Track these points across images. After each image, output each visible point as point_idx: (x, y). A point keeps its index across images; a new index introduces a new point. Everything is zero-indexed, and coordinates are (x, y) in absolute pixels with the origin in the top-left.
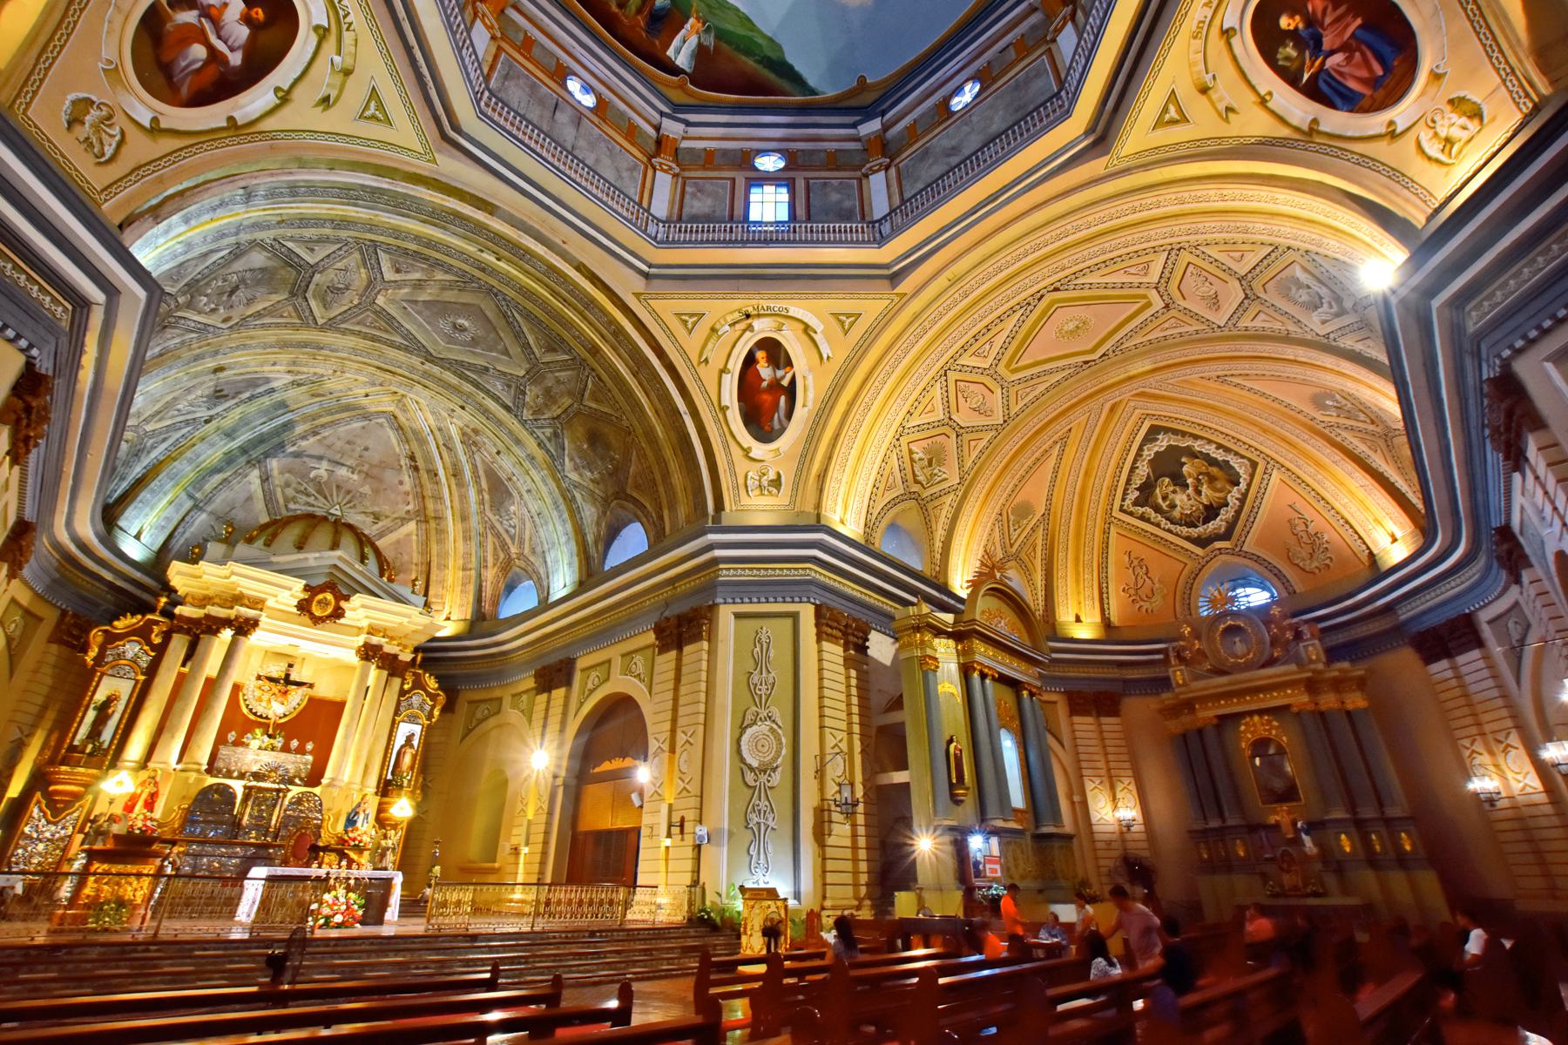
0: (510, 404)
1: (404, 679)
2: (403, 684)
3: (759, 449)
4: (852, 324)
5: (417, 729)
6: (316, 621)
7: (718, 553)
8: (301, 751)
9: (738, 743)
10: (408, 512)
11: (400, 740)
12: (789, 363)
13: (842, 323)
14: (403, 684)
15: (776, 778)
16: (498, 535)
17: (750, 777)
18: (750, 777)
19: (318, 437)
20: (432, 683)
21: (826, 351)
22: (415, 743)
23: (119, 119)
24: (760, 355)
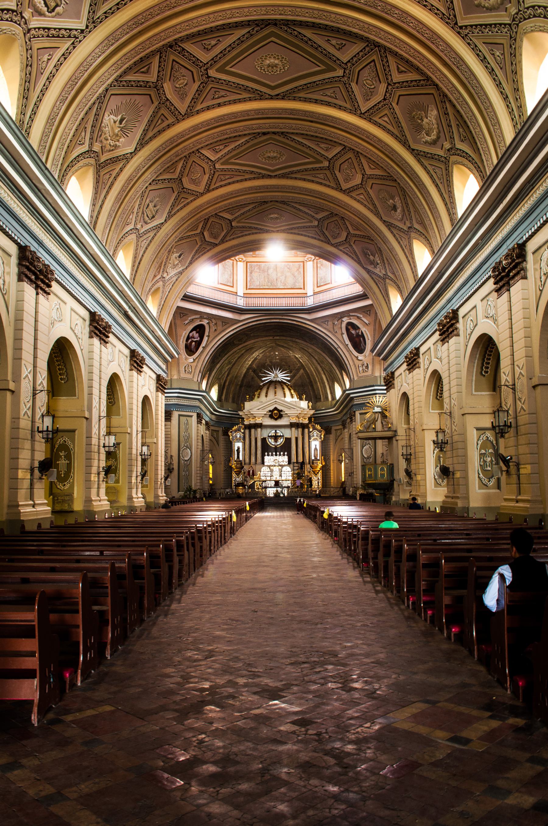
1: (309, 428)
3: (361, 357)
4: (370, 313)
6: (276, 419)
7: (352, 396)
8: (284, 455)
9: (362, 451)
11: (313, 448)
12: (359, 328)
13: (367, 313)
15: (371, 460)
16: (327, 371)
17: (365, 460)
18: (365, 460)
20: (318, 427)
21: (367, 322)
23: (190, 364)
24: (349, 327)
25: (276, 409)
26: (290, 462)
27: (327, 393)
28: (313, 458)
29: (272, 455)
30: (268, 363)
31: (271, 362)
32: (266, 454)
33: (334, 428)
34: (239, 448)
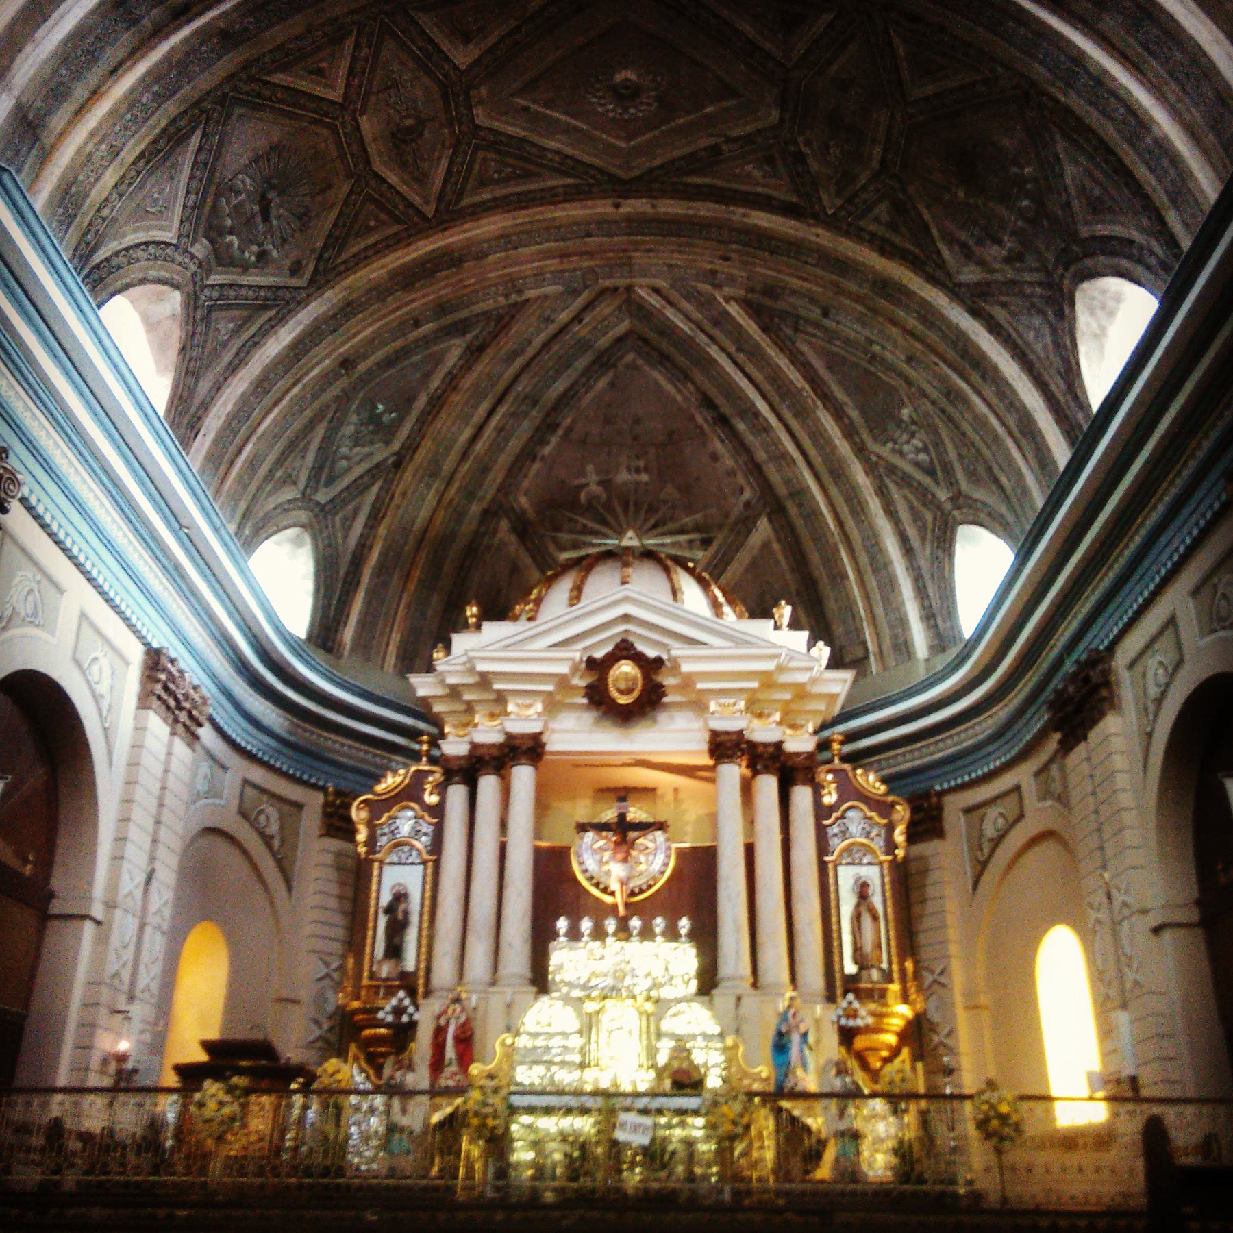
0: (794, 199)
2: (817, 797)
5: (872, 874)
8: (672, 934)
10: (747, 504)
14: (817, 797)
16: (905, 481)
19: (560, 432)
22: (877, 901)
25: (624, 650)
26: (708, 981)
27: (903, 622)
28: (850, 968)
29: (599, 934)
30: (594, 488)
31: (606, 484)
32: (562, 924)
33: (953, 806)
34: (400, 897)
